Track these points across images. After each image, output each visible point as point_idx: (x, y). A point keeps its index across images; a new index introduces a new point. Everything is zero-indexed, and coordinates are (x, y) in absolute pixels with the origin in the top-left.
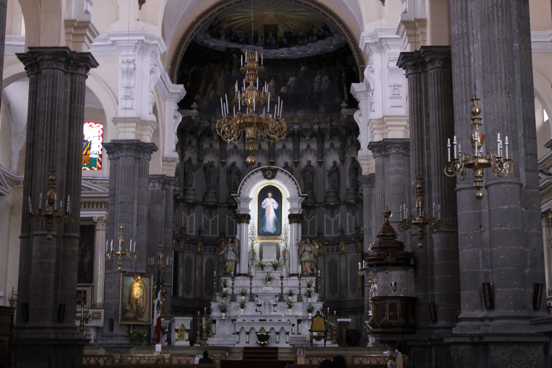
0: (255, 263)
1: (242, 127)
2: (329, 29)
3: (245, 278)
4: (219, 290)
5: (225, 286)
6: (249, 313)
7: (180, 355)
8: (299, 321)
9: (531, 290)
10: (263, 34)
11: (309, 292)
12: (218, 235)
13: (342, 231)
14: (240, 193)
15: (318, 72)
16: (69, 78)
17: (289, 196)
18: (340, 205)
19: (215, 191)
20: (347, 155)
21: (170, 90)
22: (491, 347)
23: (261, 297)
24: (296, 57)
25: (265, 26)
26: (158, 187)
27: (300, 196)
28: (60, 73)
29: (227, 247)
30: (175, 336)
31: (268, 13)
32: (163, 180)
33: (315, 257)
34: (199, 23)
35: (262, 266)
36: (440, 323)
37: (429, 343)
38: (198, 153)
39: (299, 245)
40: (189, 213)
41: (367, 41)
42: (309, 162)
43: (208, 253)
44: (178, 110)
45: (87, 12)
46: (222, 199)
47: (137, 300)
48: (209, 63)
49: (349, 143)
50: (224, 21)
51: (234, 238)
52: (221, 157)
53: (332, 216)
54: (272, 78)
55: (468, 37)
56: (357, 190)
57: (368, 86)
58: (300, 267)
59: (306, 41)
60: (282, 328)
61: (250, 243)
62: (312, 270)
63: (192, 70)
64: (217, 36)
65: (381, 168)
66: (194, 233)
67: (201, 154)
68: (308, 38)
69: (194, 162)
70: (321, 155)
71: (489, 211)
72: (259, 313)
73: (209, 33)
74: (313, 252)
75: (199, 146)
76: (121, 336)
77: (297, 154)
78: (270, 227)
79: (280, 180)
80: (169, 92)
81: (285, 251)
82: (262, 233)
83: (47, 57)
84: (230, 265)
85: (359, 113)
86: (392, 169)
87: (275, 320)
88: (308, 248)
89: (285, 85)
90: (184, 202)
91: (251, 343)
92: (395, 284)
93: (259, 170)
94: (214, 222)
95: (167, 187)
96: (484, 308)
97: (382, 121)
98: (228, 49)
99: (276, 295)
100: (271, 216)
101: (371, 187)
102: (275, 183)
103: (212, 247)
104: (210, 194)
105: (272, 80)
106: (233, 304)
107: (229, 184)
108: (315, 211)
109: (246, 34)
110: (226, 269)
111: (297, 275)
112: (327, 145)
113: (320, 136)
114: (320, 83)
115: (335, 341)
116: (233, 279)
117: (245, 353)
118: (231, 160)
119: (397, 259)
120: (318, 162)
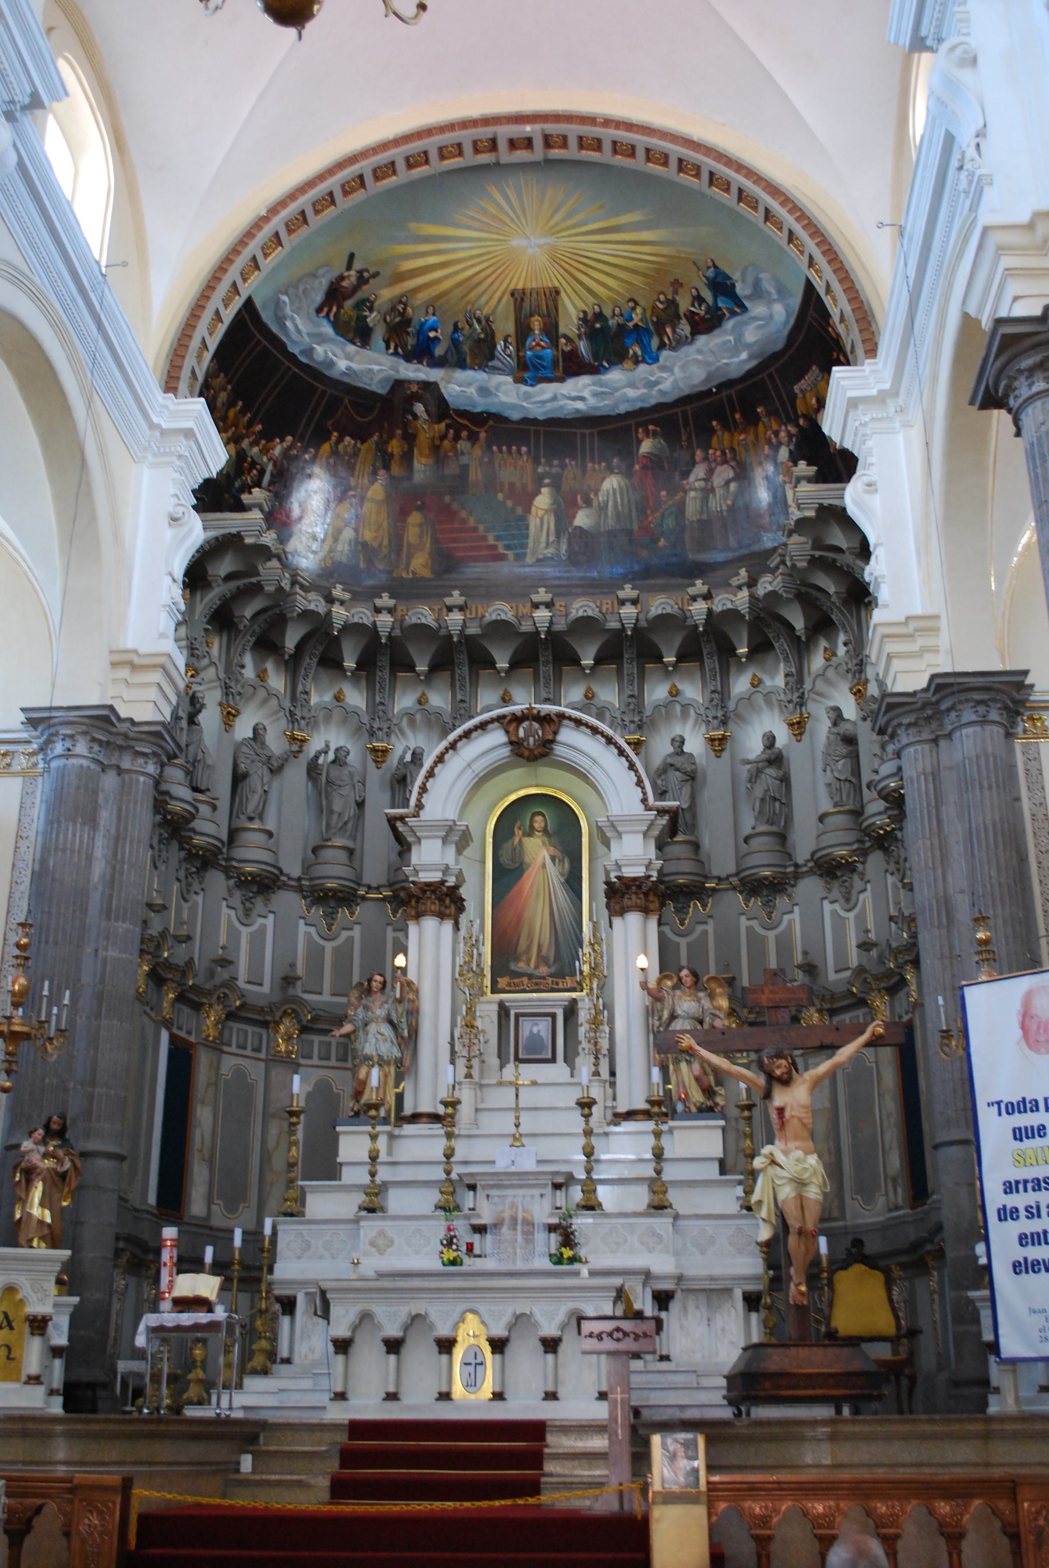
2: (733, 286)
3: (437, 1129)
10: (510, 328)
13: (810, 969)
14: (420, 806)
15: (699, 453)
18: (797, 876)
19: (350, 844)
20: (811, 707)
21: (155, 420)
23: (493, 1192)
24: (622, 409)
25: (519, 297)
27: (648, 808)
29: (366, 1008)
31: (524, 242)
42: (679, 743)
43: (315, 1061)
46: (374, 872)
48: (335, 434)
50: (376, 275)
52: (372, 734)
54: (547, 481)
59: (655, 342)
63: (277, 451)
66: (266, 988)
68: (661, 333)
69: (275, 743)
70: (720, 714)
73: (327, 316)
74: (707, 1020)
75: (296, 696)
80: (152, 426)
85: (865, 479)
88: (686, 1005)
89: (588, 503)
90: (227, 871)
91: (406, 1400)
93: (492, 721)
94: (343, 955)
98: (399, 385)
99: (560, 1180)
101: (935, 741)
104: (327, 854)
105: (545, 490)
108: (704, 906)
109: (456, 328)
117: (348, 1457)
120: (712, 740)
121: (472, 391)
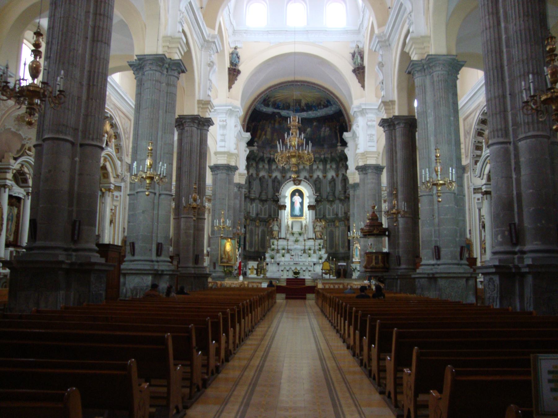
0: (289, 232)
1: (289, 158)
3: (284, 240)
4: (270, 247)
5: (273, 245)
6: (287, 260)
7: (253, 282)
8: (314, 264)
9: (459, 249)
11: (320, 248)
12: (267, 216)
13: (337, 215)
16: (199, 131)
17: (308, 195)
22: (439, 280)
24: (311, 117)
26: (236, 189)
28: (195, 129)
30: (249, 272)
32: (239, 186)
33: (322, 229)
34: (259, 99)
35: (293, 234)
36: (403, 266)
37: (396, 277)
38: (257, 170)
39: (314, 222)
40: (251, 204)
41: (355, 110)
42: (318, 176)
44: (247, 147)
45: (209, 96)
46: (270, 196)
47: (228, 252)
49: (341, 165)
51: (277, 218)
52: (269, 173)
53: (331, 206)
55: (426, 113)
56: (345, 192)
57: (354, 133)
58: (314, 234)
59: (317, 108)
60: (307, 268)
61: (286, 221)
62: (321, 236)
63: (253, 124)
64: (268, 105)
65: (362, 180)
67: (258, 170)
69: (254, 176)
71: (438, 208)
72: (292, 260)
76: (220, 272)
77: (311, 171)
78: (297, 212)
79: (304, 186)
81: (306, 226)
82: (293, 215)
83: (188, 120)
84: (275, 233)
86: (369, 181)
87: (301, 264)
88: (319, 224)
92: (371, 245)
94: (265, 209)
95: (241, 189)
96: (435, 259)
97: (364, 155)
98: (274, 113)
100: (297, 206)
102: (300, 187)
103: (264, 223)
106: (278, 255)
107: (273, 188)
109: (284, 104)
110: (273, 235)
111: (313, 239)
112: (328, 166)
113: (324, 161)
114: (325, 132)
115: (334, 275)
116: (278, 240)
117: (287, 282)
118: (274, 175)
119: (380, 232)
121: (286, 114)
